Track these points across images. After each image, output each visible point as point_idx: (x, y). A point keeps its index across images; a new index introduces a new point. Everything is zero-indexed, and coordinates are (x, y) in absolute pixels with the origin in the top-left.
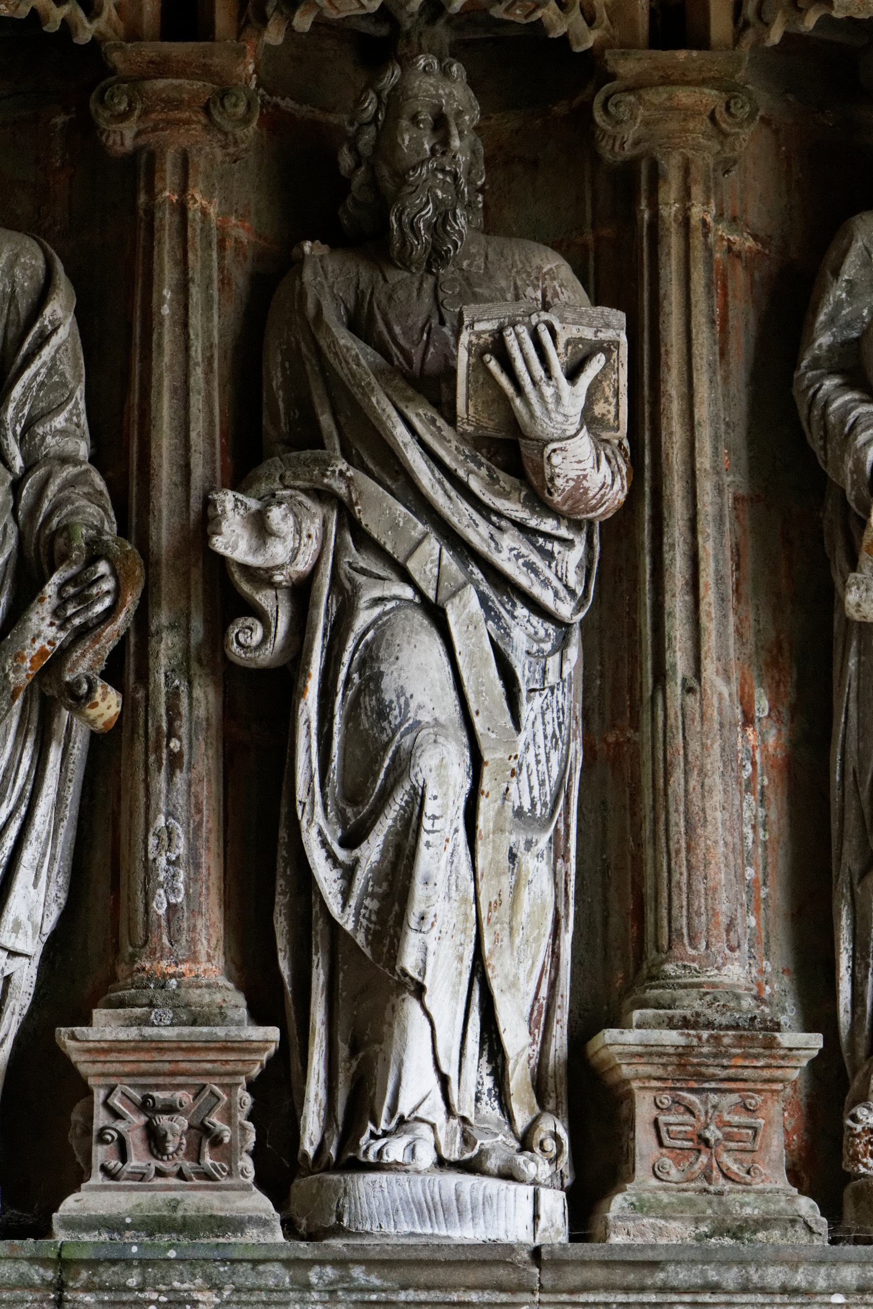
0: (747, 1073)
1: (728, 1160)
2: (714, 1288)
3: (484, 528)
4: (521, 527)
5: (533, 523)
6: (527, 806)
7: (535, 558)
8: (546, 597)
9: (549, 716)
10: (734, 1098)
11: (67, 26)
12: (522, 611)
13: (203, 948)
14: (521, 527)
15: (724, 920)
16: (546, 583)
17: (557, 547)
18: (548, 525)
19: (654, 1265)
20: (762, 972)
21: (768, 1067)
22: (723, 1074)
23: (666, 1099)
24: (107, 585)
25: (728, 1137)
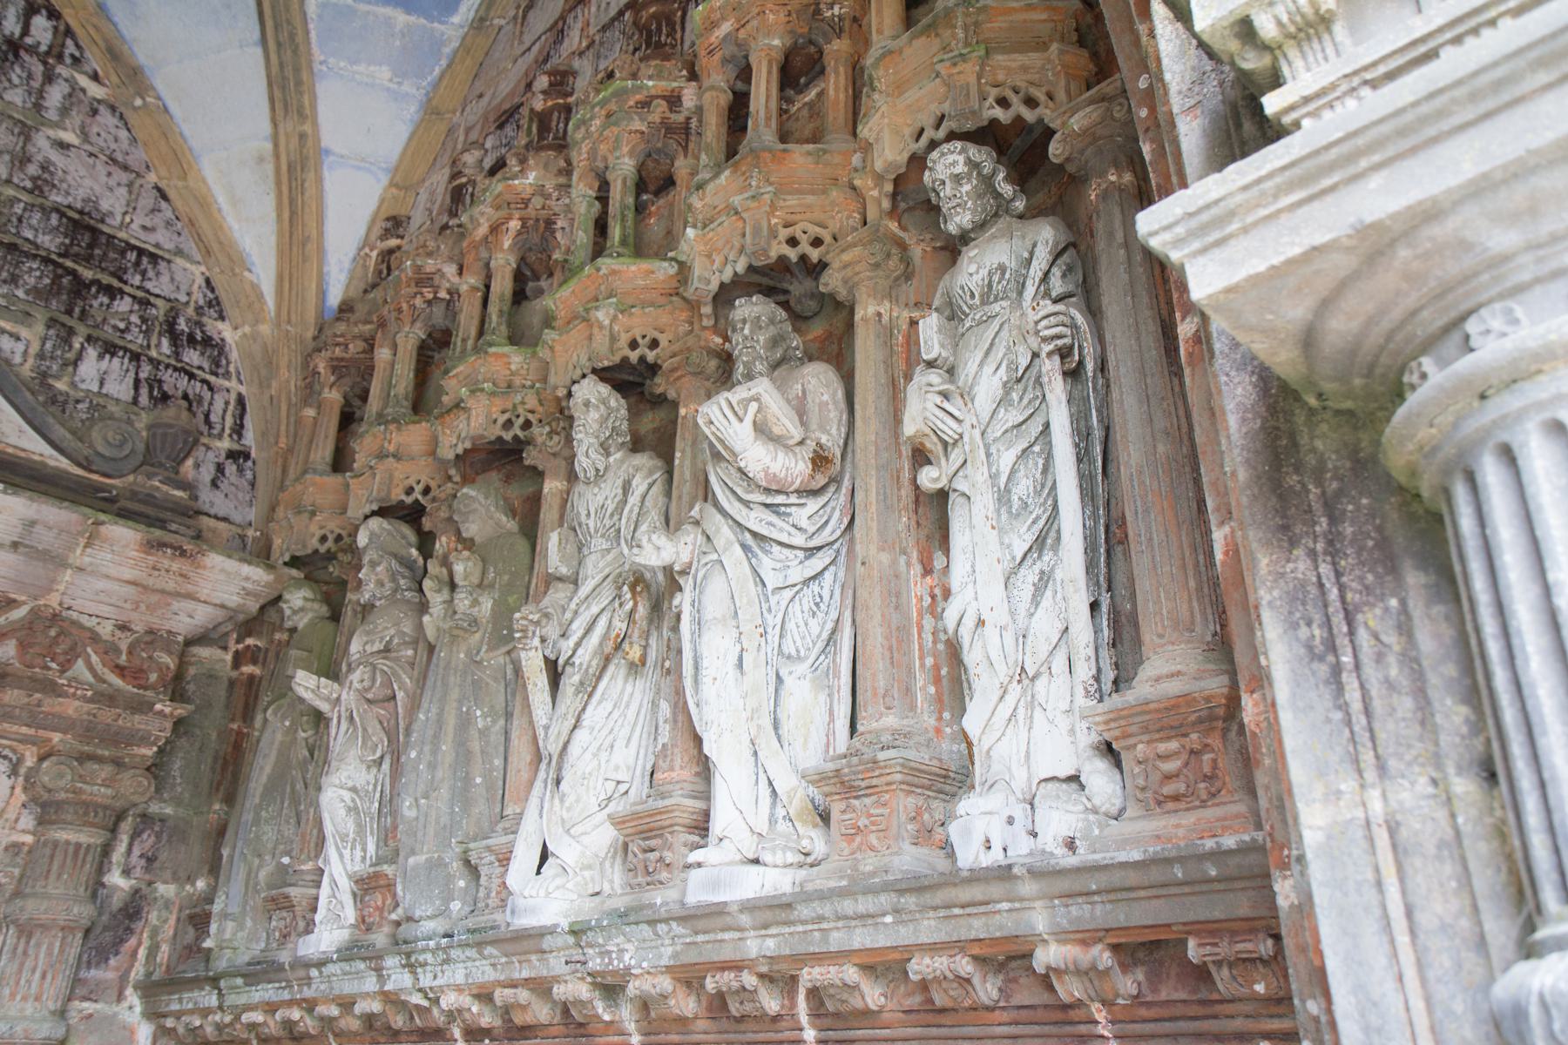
0: (875, 782)
1: (873, 839)
2: (821, 919)
3: (745, 511)
4: (767, 506)
5: (769, 501)
6: (794, 653)
7: (773, 519)
8: (784, 538)
9: (805, 601)
10: (874, 798)
11: (642, 359)
12: (776, 549)
13: (678, 762)
14: (767, 506)
15: (882, 691)
16: (781, 530)
17: (793, 509)
18: (780, 499)
19: (789, 906)
20: (940, 719)
21: (881, 775)
22: (863, 784)
23: (842, 806)
24: (629, 596)
25: (873, 823)
